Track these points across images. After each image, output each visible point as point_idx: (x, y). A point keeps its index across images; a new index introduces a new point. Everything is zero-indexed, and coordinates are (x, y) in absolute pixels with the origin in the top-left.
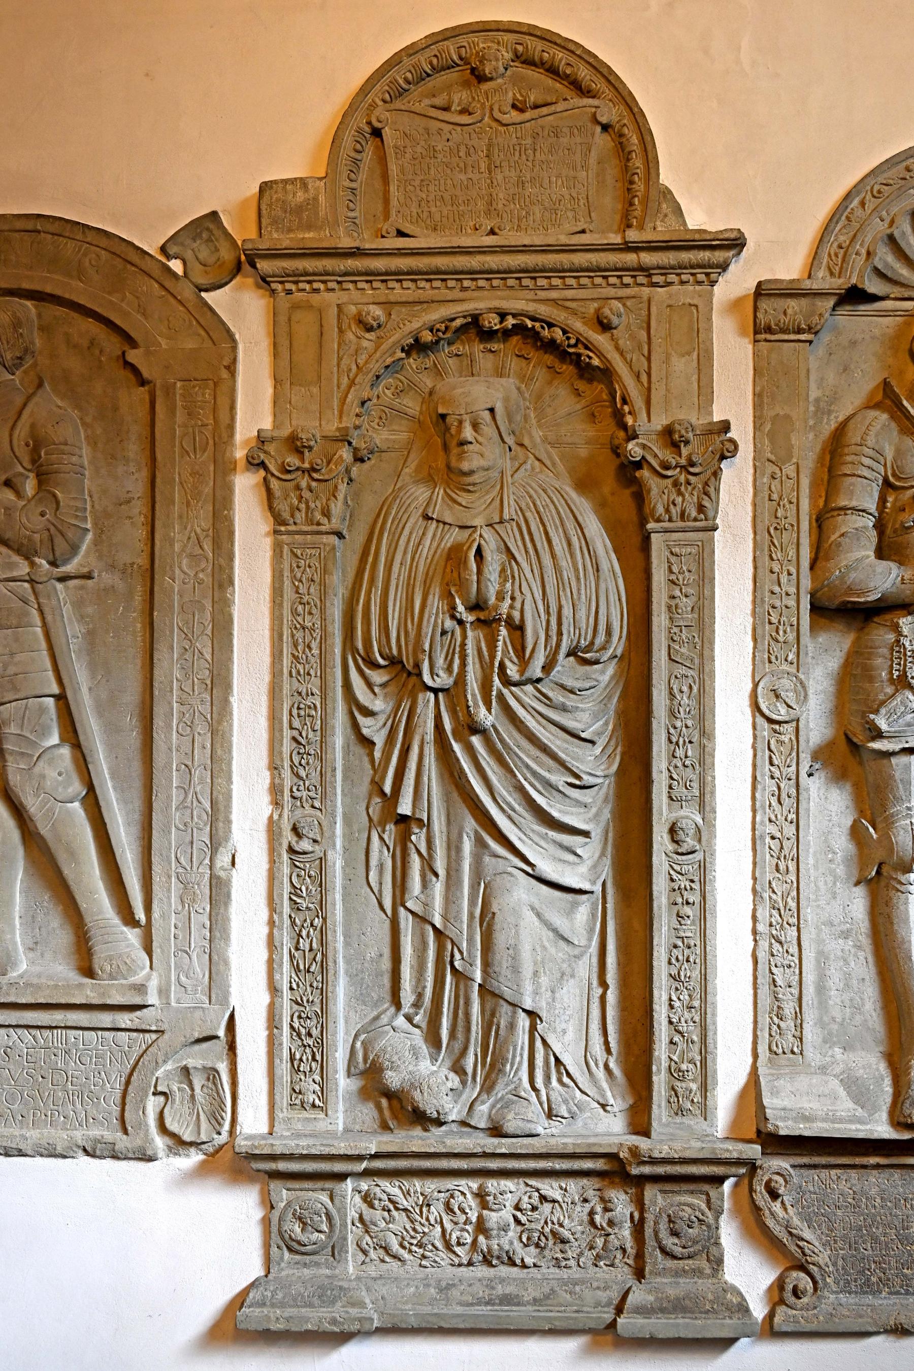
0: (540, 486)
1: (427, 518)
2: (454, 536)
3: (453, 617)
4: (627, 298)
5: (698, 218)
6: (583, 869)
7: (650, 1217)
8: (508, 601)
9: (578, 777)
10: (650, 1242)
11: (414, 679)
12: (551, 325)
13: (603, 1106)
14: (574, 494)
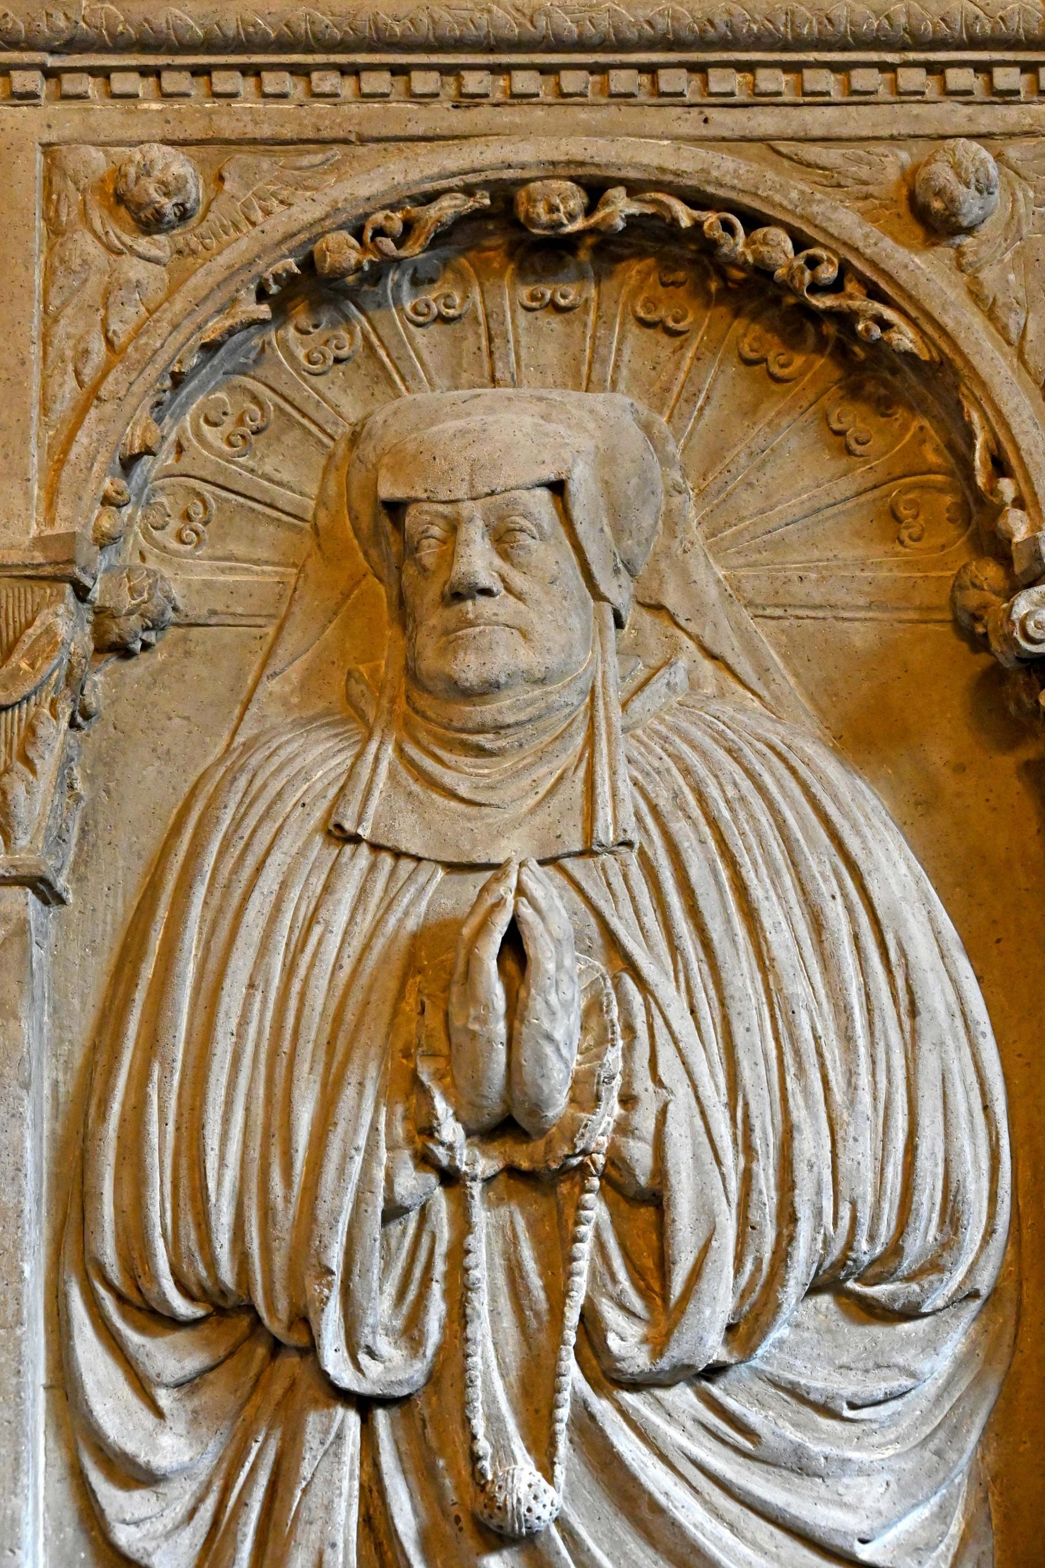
0: (719, 738)
1: (340, 836)
2: (427, 898)
3: (424, 1160)
4: (1010, 135)
8: (611, 1110)
11: (290, 1363)
12: (753, 220)
14: (832, 768)
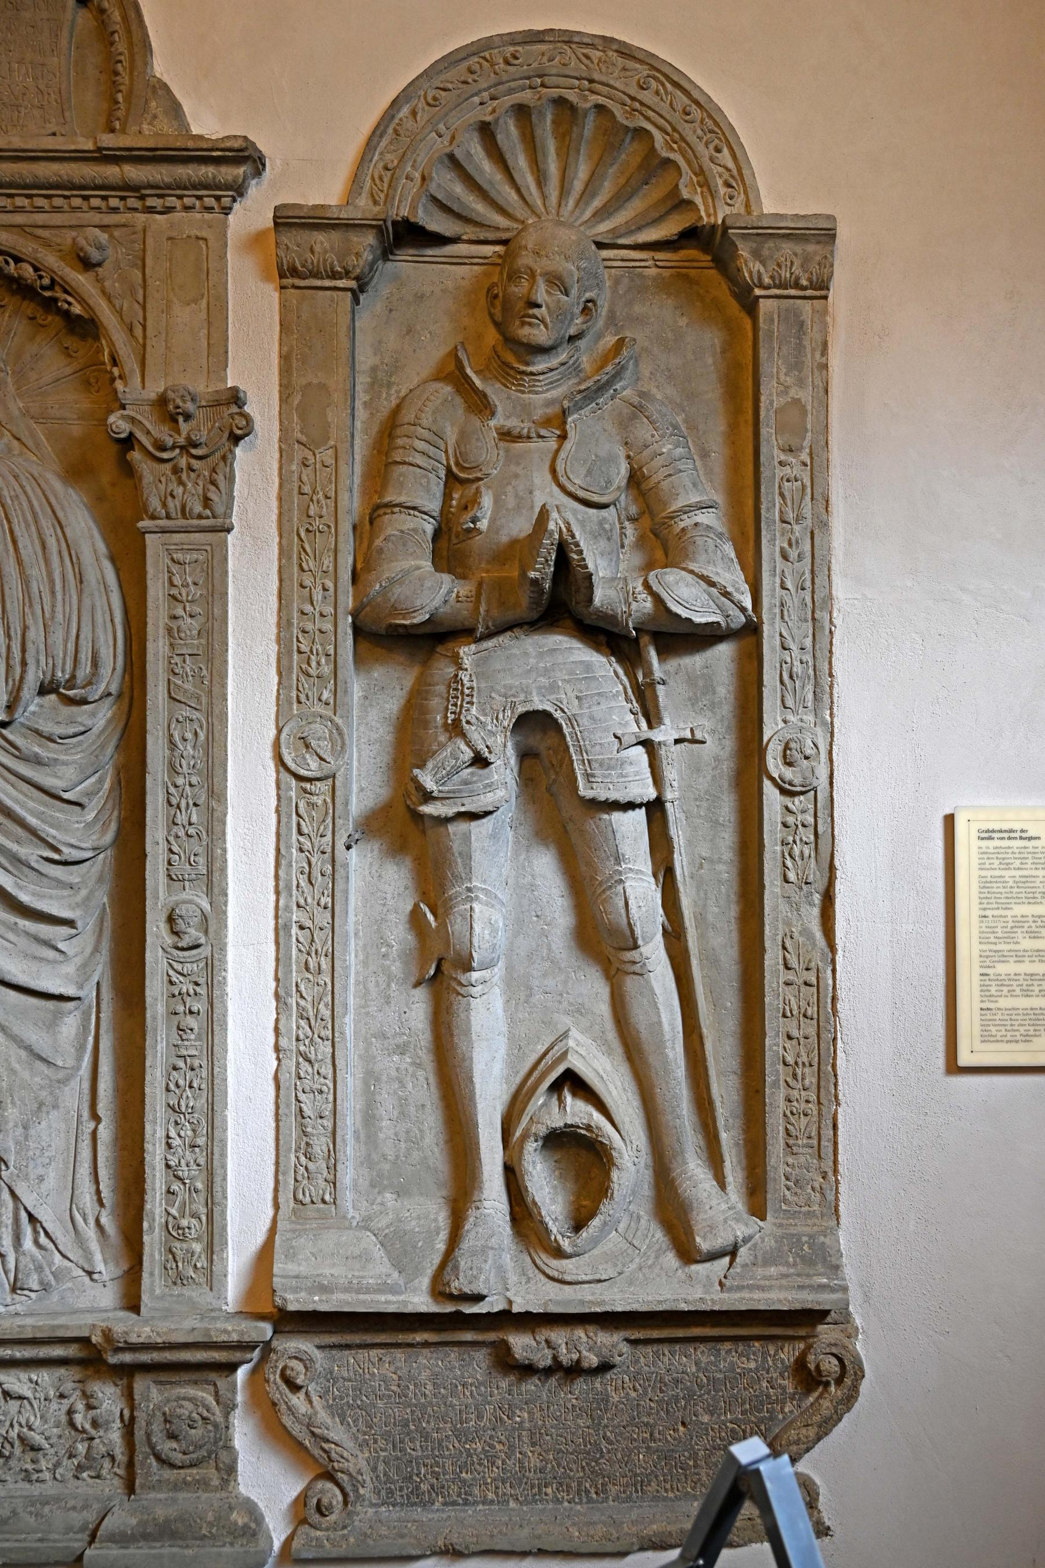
0: (11, 471)
4: (117, 226)
5: (206, 124)
6: (69, 969)
7: (141, 1417)
9: (57, 850)
10: (141, 1448)
12: (17, 260)
13: (90, 1274)
14: (58, 485)
